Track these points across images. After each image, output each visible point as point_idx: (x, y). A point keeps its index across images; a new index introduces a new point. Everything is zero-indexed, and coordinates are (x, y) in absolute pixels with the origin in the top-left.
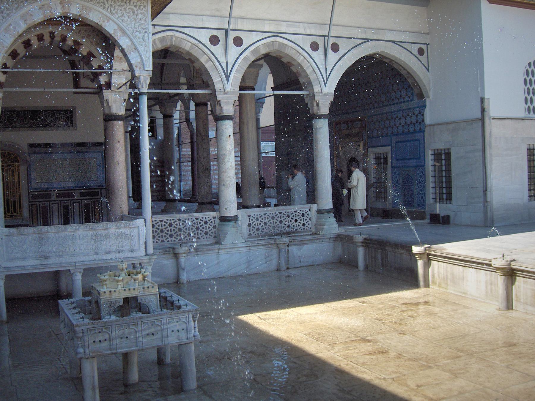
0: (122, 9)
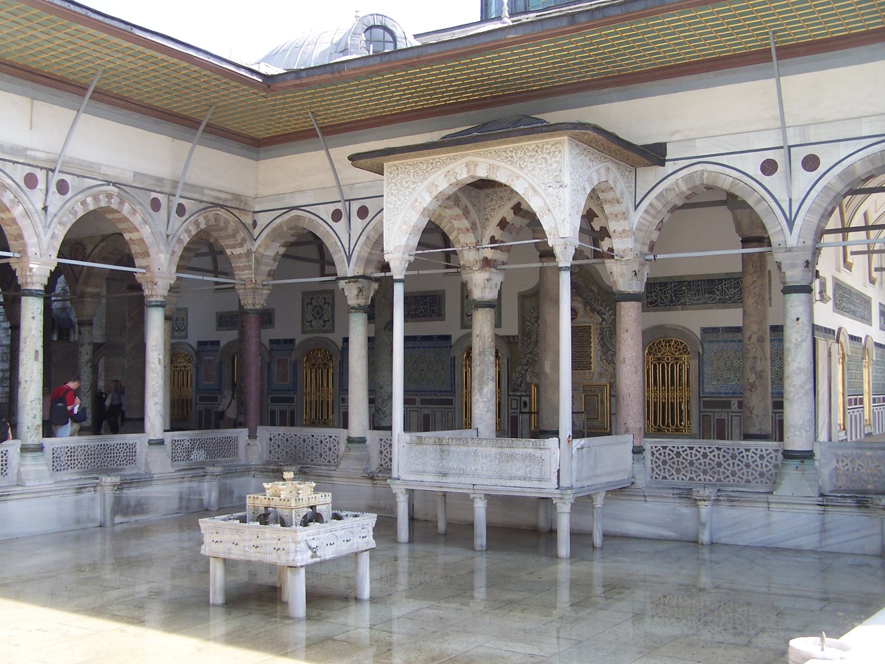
0: (533, 160)
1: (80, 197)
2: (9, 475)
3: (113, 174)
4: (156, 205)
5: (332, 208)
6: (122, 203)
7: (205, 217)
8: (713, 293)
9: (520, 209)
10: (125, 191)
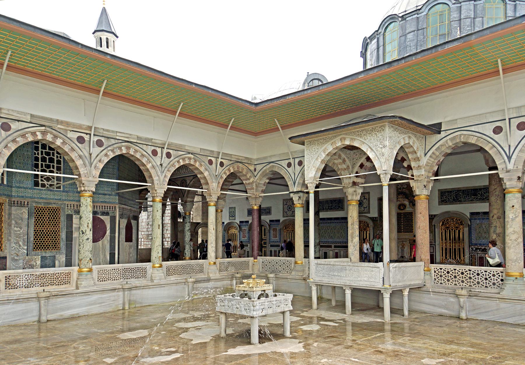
1: (177, 159)
3: (191, 149)
4: (210, 162)
5: (287, 162)
6: (195, 161)
7: (233, 167)
8: (477, 195)
9: (368, 159)
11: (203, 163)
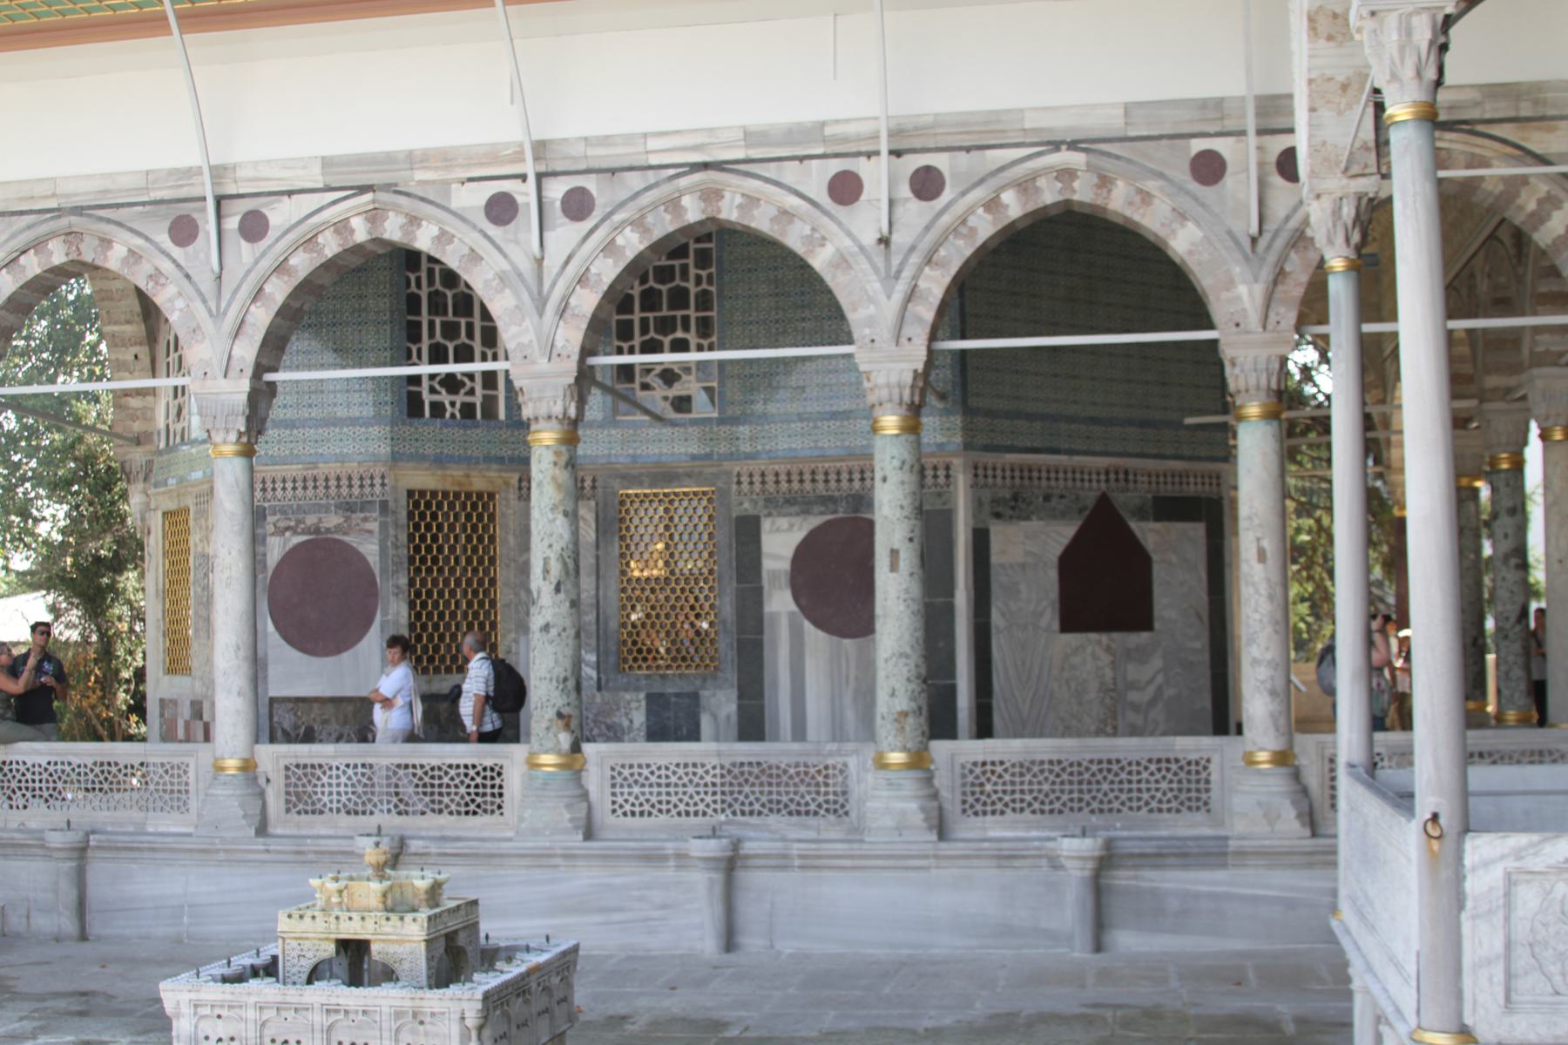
1: (979, 194)
2: (853, 815)
3: (1061, 124)
6: (1105, 182)
10: (1109, 155)
11: (1151, 185)
